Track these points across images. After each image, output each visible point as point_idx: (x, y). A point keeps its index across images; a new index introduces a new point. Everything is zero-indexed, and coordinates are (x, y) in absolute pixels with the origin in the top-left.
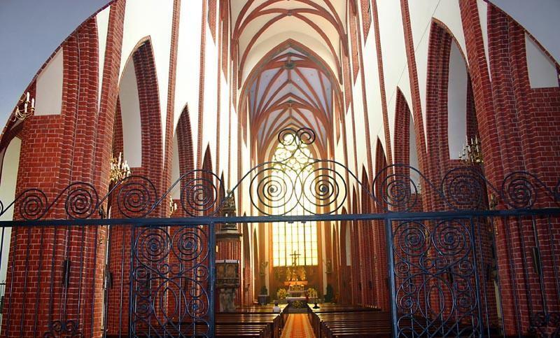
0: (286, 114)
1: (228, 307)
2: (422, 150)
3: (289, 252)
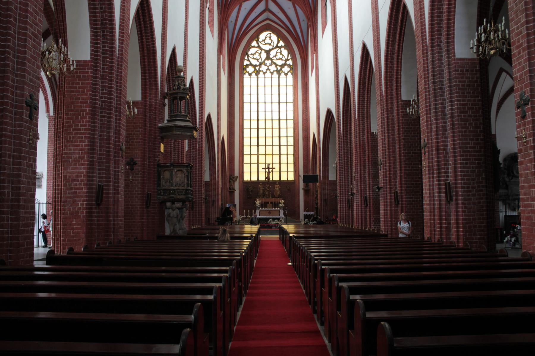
0: (261, 7)
1: (177, 226)
3: (262, 166)
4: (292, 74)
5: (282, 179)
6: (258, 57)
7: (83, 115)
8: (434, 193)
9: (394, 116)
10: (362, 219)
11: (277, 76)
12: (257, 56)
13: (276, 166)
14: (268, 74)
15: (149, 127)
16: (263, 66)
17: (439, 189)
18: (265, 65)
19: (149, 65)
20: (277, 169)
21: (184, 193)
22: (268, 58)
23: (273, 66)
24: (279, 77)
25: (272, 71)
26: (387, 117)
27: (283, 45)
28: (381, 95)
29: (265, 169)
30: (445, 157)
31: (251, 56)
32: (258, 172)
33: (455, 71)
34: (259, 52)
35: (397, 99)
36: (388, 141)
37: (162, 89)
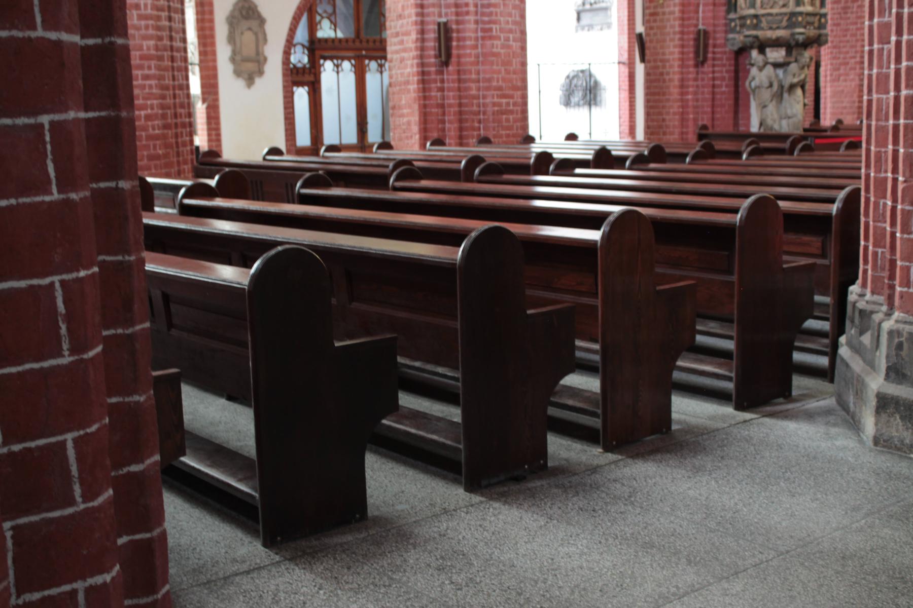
21: (784, 23)
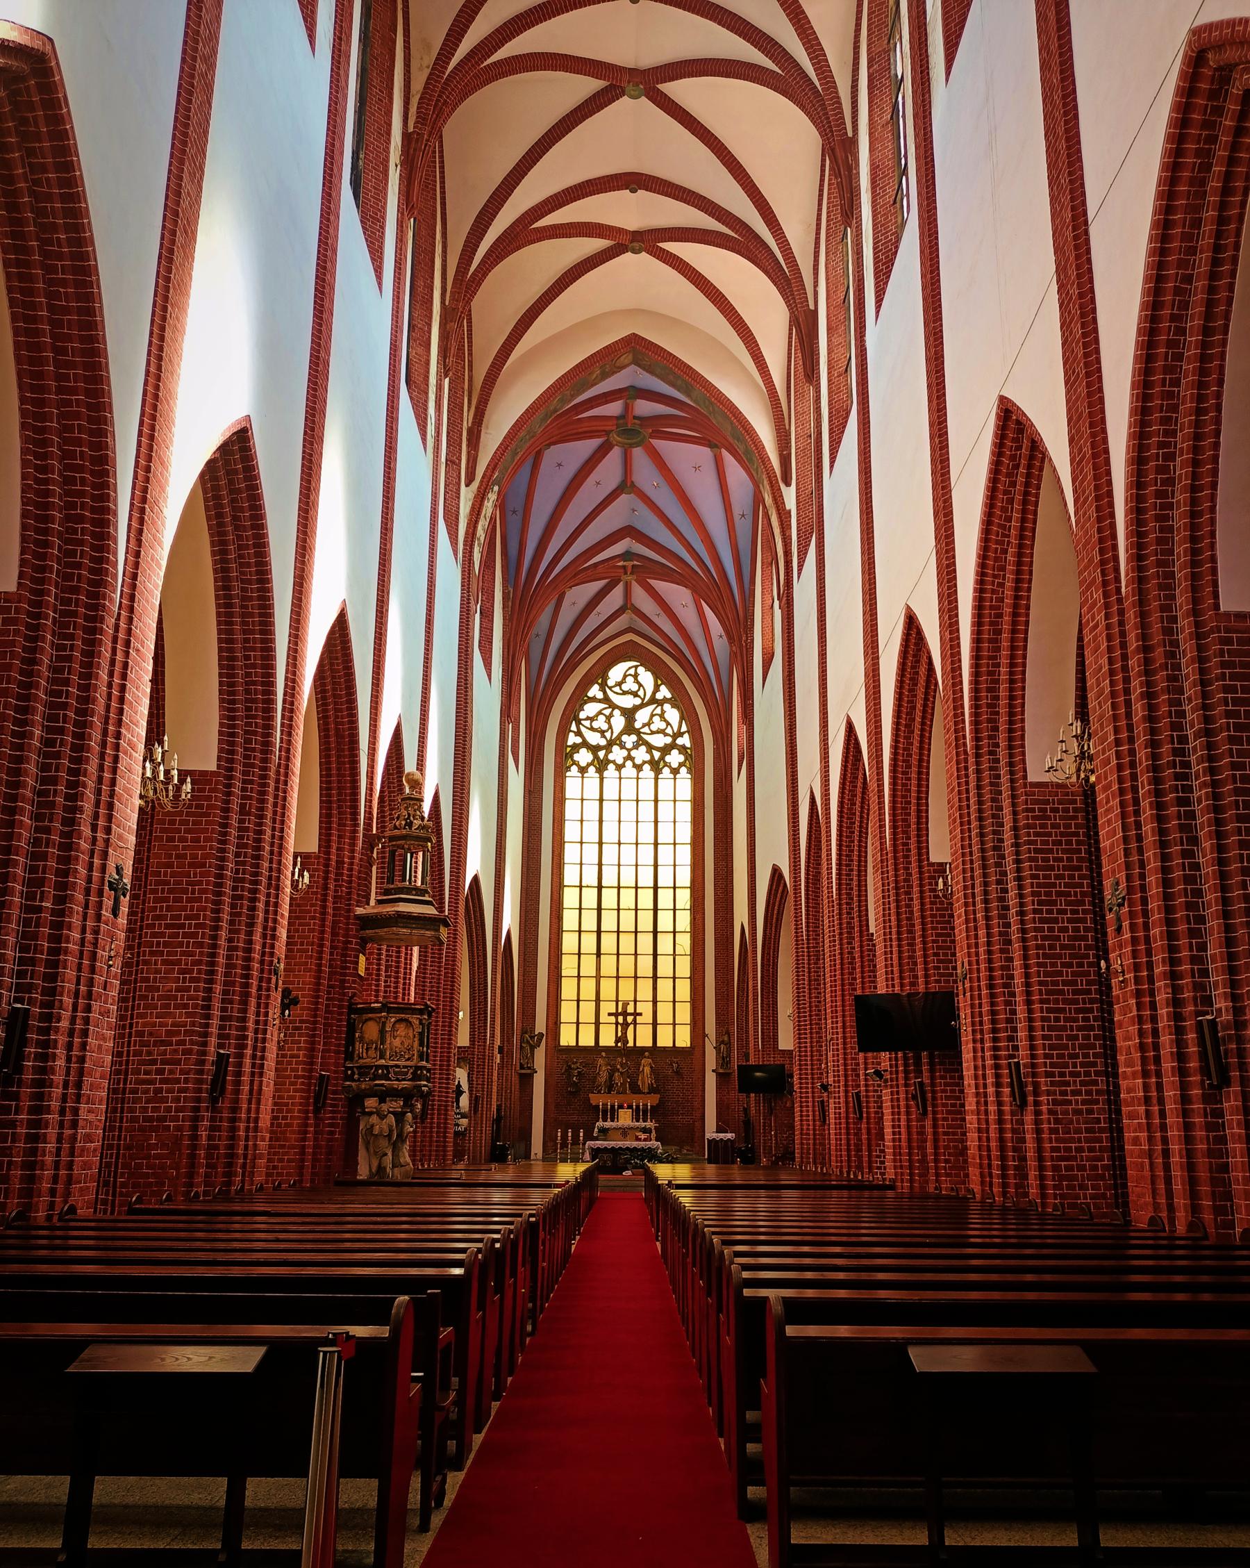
2: (1105, 583)
3: (607, 1007)
4: (690, 771)
5: (659, 1044)
6: (605, 727)
7: (193, 893)
8: (985, 1086)
9: (911, 899)
10: (848, 1150)
11: (652, 774)
12: (601, 723)
13: (645, 1009)
14: (629, 770)
15: (334, 915)
16: (616, 748)
17: (997, 1076)
18: (622, 746)
19: (338, 769)
20: (647, 1017)
21: (410, 1076)
22: (629, 728)
23: (643, 748)
24: (656, 779)
25: (638, 762)
26: (897, 901)
27: (669, 696)
28: (882, 850)
29: (616, 1015)
30: (1008, 1003)
31: (587, 723)
32: (597, 1024)
33: (1027, 810)
34: (607, 712)
35: (920, 861)
36: (900, 958)
37: (368, 825)
